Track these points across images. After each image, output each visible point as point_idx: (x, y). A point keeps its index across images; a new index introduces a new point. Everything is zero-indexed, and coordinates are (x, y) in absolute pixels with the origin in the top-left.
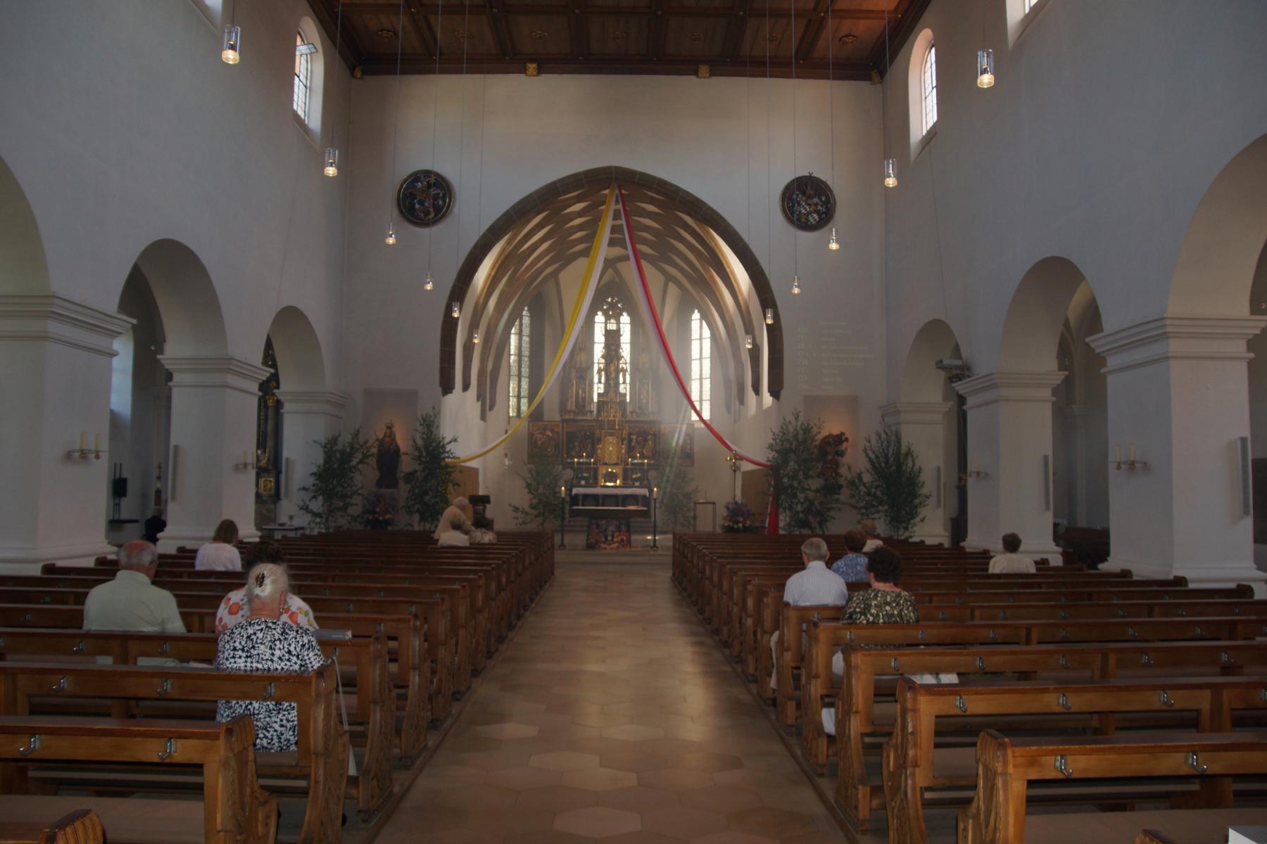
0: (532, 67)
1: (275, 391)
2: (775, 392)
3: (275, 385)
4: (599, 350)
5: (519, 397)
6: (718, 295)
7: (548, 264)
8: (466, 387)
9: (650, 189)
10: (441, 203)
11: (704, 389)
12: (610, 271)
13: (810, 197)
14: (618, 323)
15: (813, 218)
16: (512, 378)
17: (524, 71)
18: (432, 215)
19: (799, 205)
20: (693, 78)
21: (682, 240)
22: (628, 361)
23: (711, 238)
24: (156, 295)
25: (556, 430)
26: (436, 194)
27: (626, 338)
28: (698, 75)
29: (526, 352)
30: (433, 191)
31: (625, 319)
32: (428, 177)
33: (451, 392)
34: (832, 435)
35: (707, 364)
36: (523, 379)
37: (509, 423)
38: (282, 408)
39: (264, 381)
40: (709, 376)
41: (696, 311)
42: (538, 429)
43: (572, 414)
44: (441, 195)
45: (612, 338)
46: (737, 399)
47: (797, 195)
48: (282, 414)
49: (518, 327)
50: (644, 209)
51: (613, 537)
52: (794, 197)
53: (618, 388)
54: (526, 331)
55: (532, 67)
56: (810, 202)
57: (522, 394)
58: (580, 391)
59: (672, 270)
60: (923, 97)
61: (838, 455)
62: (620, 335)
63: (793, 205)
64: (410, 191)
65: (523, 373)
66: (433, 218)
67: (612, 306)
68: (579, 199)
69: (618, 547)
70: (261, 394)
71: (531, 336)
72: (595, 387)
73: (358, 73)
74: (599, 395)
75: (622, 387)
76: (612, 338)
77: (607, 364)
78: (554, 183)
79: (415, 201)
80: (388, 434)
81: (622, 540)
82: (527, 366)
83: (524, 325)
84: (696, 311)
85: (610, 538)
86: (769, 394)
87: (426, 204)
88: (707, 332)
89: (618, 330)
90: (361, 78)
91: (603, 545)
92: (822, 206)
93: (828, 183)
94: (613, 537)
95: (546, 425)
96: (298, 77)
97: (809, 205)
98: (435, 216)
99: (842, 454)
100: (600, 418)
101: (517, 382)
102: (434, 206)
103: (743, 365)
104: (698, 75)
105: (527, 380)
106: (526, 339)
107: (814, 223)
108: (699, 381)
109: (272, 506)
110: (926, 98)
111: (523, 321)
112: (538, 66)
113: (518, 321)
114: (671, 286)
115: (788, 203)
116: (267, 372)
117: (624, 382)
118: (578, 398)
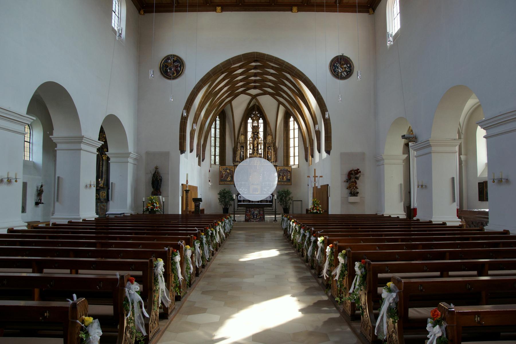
0: (219, 8)
1: (106, 153)
2: (328, 152)
3: (107, 150)
4: (250, 135)
5: (215, 156)
6: (302, 109)
7: (227, 97)
8: (191, 151)
9: (271, 62)
10: (179, 69)
12: (254, 100)
13: (343, 65)
14: (258, 123)
15: (344, 74)
17: (215, 10)
18: (175, 75)
19: (338, 68)
20: (290, 12)
21: (286, 85)
22: (262, 140)
23: (299, 84)
24: (49, 110)
25: (231, 170)
26: (177, 65)
27: (261, 129)
28: (292, 11)
29: (218, 136)
30: (176, 64)
31: (261, 121)
32: (174, 58)
33: (184, 153)
34: (354, 170)
35: (297, 140)
36: (217, 148)
37: (211, 167)
38: (110, 160)
39: (99, 148)
41: (292, 117)
42: (223, 169)
43: (238, 162)
44: (179, 66)
45: (255, 129)
47: (337, 64)
48: (110, 163)
49: (214, 125)
50: (269, 72)
51: (257, 216)
52: (336, 64)
53: (258, 151)
54: (218, 126)
55: (219, 8)
56: (343, 67)
57: (216, 154)
58: (242, 153)
59: (281, 100)
60: (393, 19)
61: (356, 179)
62: (259, 128)
63: (335, 68)
64: (166, 64)
65: (217, 145)
66: (176, 76)
67: (255, 115)
68: (240, 67)
69: (259, 221)
70: (98, 153)
71: (220, 129)
72: (248, 150)
73: (142, 12)
74: (250, 154)
75: (260, 150)
76: (255, 129)
77: (253, 141)
78: (229, 60)
79: (168, 68)
80: (157, 172)
81: (261, 218)
82: (218, 142)
83: (217, 124)
84: (292, 117)
85: (255, 217)
86: (325, 152)
87: (172, 70)
88: (296, 126)
89: (258, 126)
90: (144, 14)
91: (252, 220)
92: (348, 69)
93: (350, 58)
94: (257, 216)
95: (227, 168)
96: (115, 13)
97: (342, 68)
98: (176, 75)
99: (357, 178)
100: (250, 164)
101: (214, 149)
102: (176, 71)
103: (313, 140)
104: (292, 11)
105: (218, 148)
106: (218, 131)
107: (344, 76)
108: (293, 148)
109: (105, 204)
110: (394, 19)
112: (222, 7)
113: (214, 122)
114: (281, 107)
115: (332, 67)
116: (100, 144)
117: (261, 149)
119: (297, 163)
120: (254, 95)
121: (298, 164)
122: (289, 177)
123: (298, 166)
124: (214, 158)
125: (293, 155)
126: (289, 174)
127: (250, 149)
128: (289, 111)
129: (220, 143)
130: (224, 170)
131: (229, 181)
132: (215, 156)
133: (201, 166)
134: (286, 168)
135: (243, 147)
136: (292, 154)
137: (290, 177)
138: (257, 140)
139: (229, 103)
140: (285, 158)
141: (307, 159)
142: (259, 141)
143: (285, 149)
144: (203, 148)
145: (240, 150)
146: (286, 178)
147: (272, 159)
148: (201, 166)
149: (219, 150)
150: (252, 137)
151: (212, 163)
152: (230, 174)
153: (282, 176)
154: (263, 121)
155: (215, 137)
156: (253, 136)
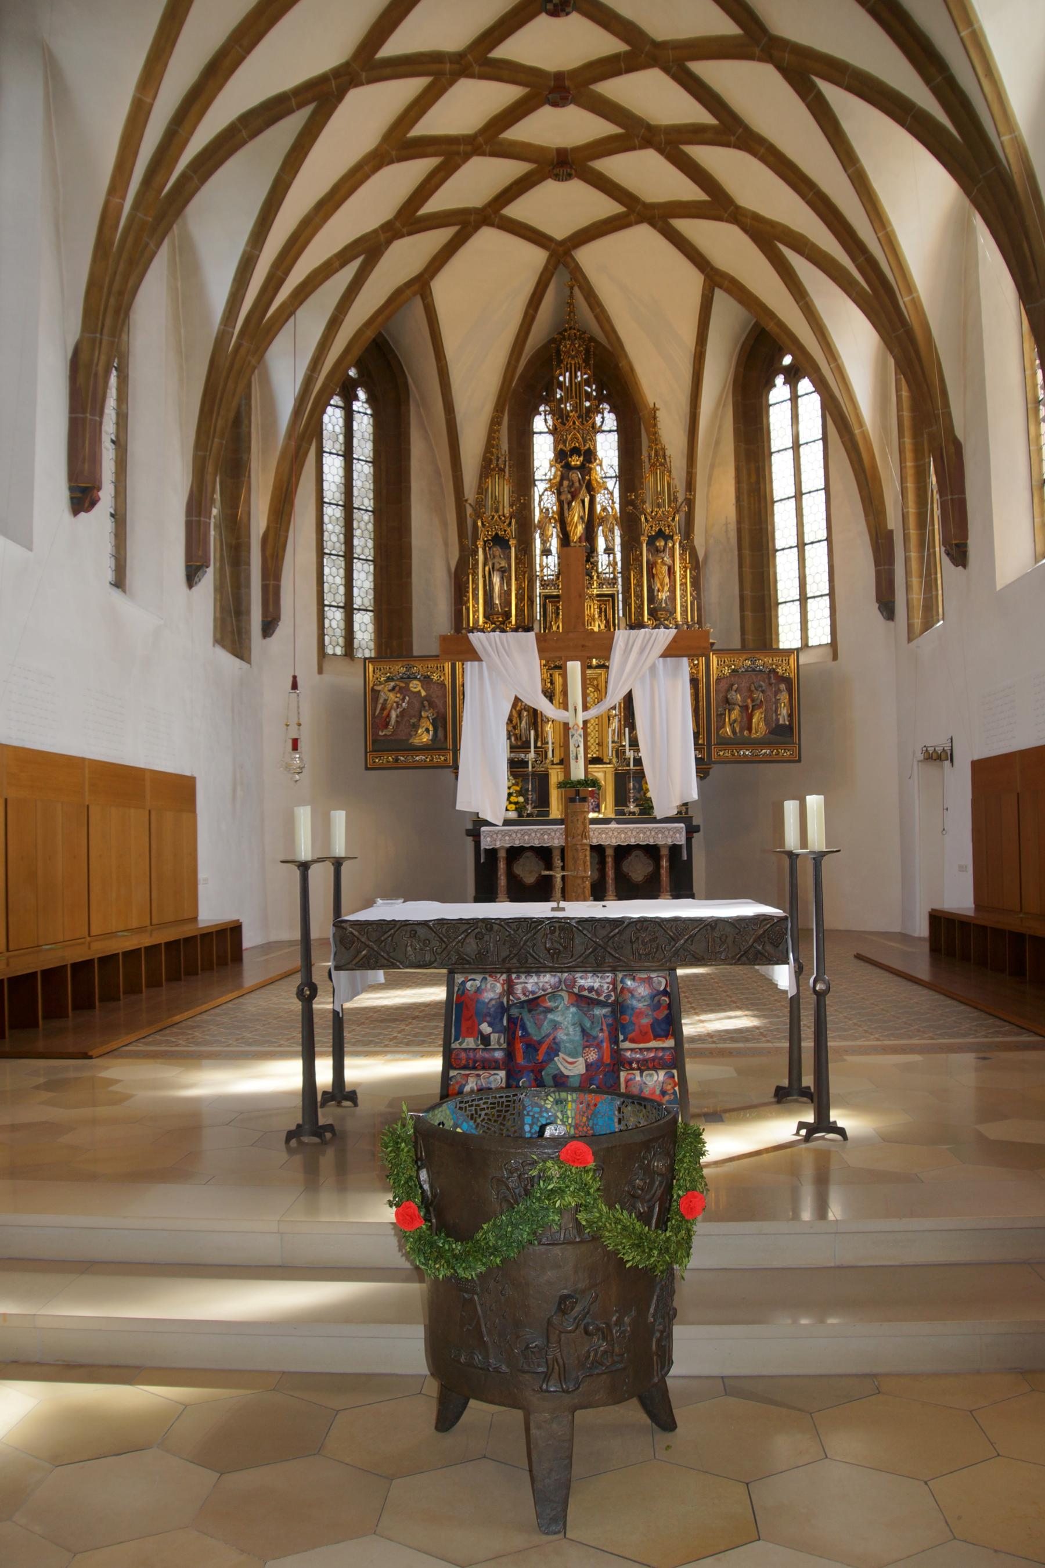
5: (349, 609)
25: (435, 677)
35: (815, 507)
36: (357, 565)
37: (320, 671)
40: (823, 534)
41: (780, 380)
42: (389, 679)
46: (943, 549)
49: (341, 438)
53: (595, 565)
54: (364, 448)
57: (357, 602)
58: (496, 579)
67: (574, 392)
71: (376, 461)
82: (366, 532)
84: (780, 380)
101: (342, 572)
106: (363, 472)
111: (355, 426)
114: (721, 298)
117: (609, 551)
118: (492, 597)
119: (820, 634)
120: (562, 243)
121: (827, 639)
122: (784, 711)
123: (829, 650)
124: (342, 625)
126: (784, 697)
127: (546, 552)
128: (771, 327)
129: (375, 540)
130: (392, 684)
131: (424, 749)
132: (349, 609)
133: (249, 662)
134: (764, 661)
135: (499, 541)
136: (786, 586)
137: (790, 716)
138: (587, 500)
139: (414, 294)
140: (748, 614)
141: (887, 608)
142: (598, 508)
143: (747, 561)
144: (268, 553)
145: (485, 565)
147: (675, 612)
148: (249, 662)
149: (371, 578)
150: (557, 487)
151: (329, 651)
152: (432, 705)
153: (745, 708)
154: (617, 420)
155: (348, 507)
156: (562, 478)
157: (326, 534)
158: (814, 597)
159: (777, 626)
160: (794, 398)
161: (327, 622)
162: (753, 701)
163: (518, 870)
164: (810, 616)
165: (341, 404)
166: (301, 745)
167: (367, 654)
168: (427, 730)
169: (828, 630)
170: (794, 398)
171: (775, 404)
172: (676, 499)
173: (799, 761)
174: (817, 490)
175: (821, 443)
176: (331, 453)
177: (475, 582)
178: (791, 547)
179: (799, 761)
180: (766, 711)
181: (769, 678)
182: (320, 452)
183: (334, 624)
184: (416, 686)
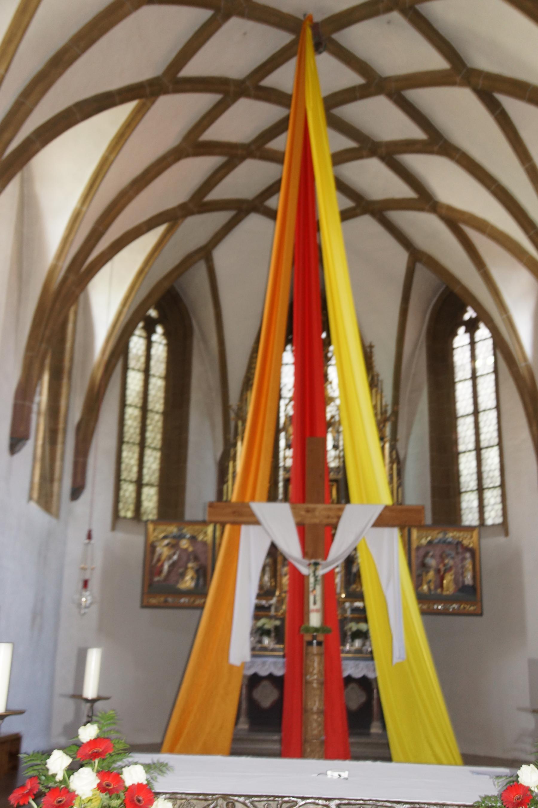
5: (139, 484)
11: (485, 468)
16: (125, 447)
25: (200, 538)
36: (148, 452)
40: (496, 441)
41: (462, 330)
42: (165, 537)
49: (143, 360)
57: (146, 479)
82: (156, 429)
84: (462, 330)
101: (136, 456)
105: (158, 454)
108: (474, 453)
111: (153, 351)
114: (421, 271)
121: (499, 520)
124: (134, 495)
125: (473, 485)
126: (468, 564)
128: (457, 290)
131: (188, 593)
132: (139, 484)
137: (474, 577)
139: (200, 259)
146: (456, 581)
151: (122, 514)
153: (438, 571)
157: (126, 429)
158: (489, 488)
159: (460, 509)
160: (473, 343)
161: (122, 493)
162: (445, 565)
163: (257, 694)
164: (486, 502)
165: (144, 334)
166: (90, 584)
167: (151, 517)
168: (192, 578)
169: (500, 513)
170: (473, 343)
171: (458, 348)
172: (386, 412)
173: (481, 615)
174: (490, 409)
175: (493, 377)
176: (133, 369)
177: (234, 467)
178: (470, 451)
179: (481, 615)
180: (456, 574)
181: (457, 548)
182: (126, 368)
183: (127, 494)
184: (184, 544)
